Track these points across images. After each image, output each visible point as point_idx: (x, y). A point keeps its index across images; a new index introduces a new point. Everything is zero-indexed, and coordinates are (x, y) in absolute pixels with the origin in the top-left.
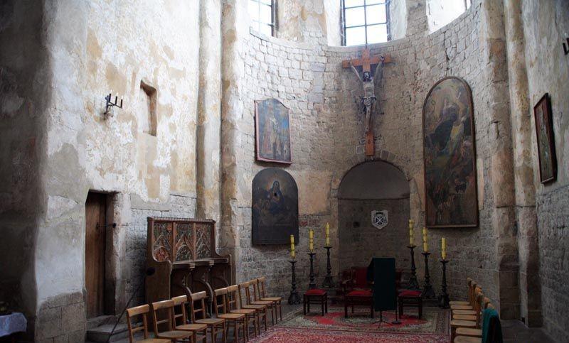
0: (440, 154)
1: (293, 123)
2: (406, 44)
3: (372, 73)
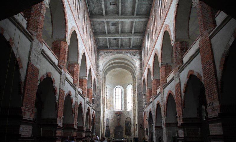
1: (109, 121)
2: (123, 111)
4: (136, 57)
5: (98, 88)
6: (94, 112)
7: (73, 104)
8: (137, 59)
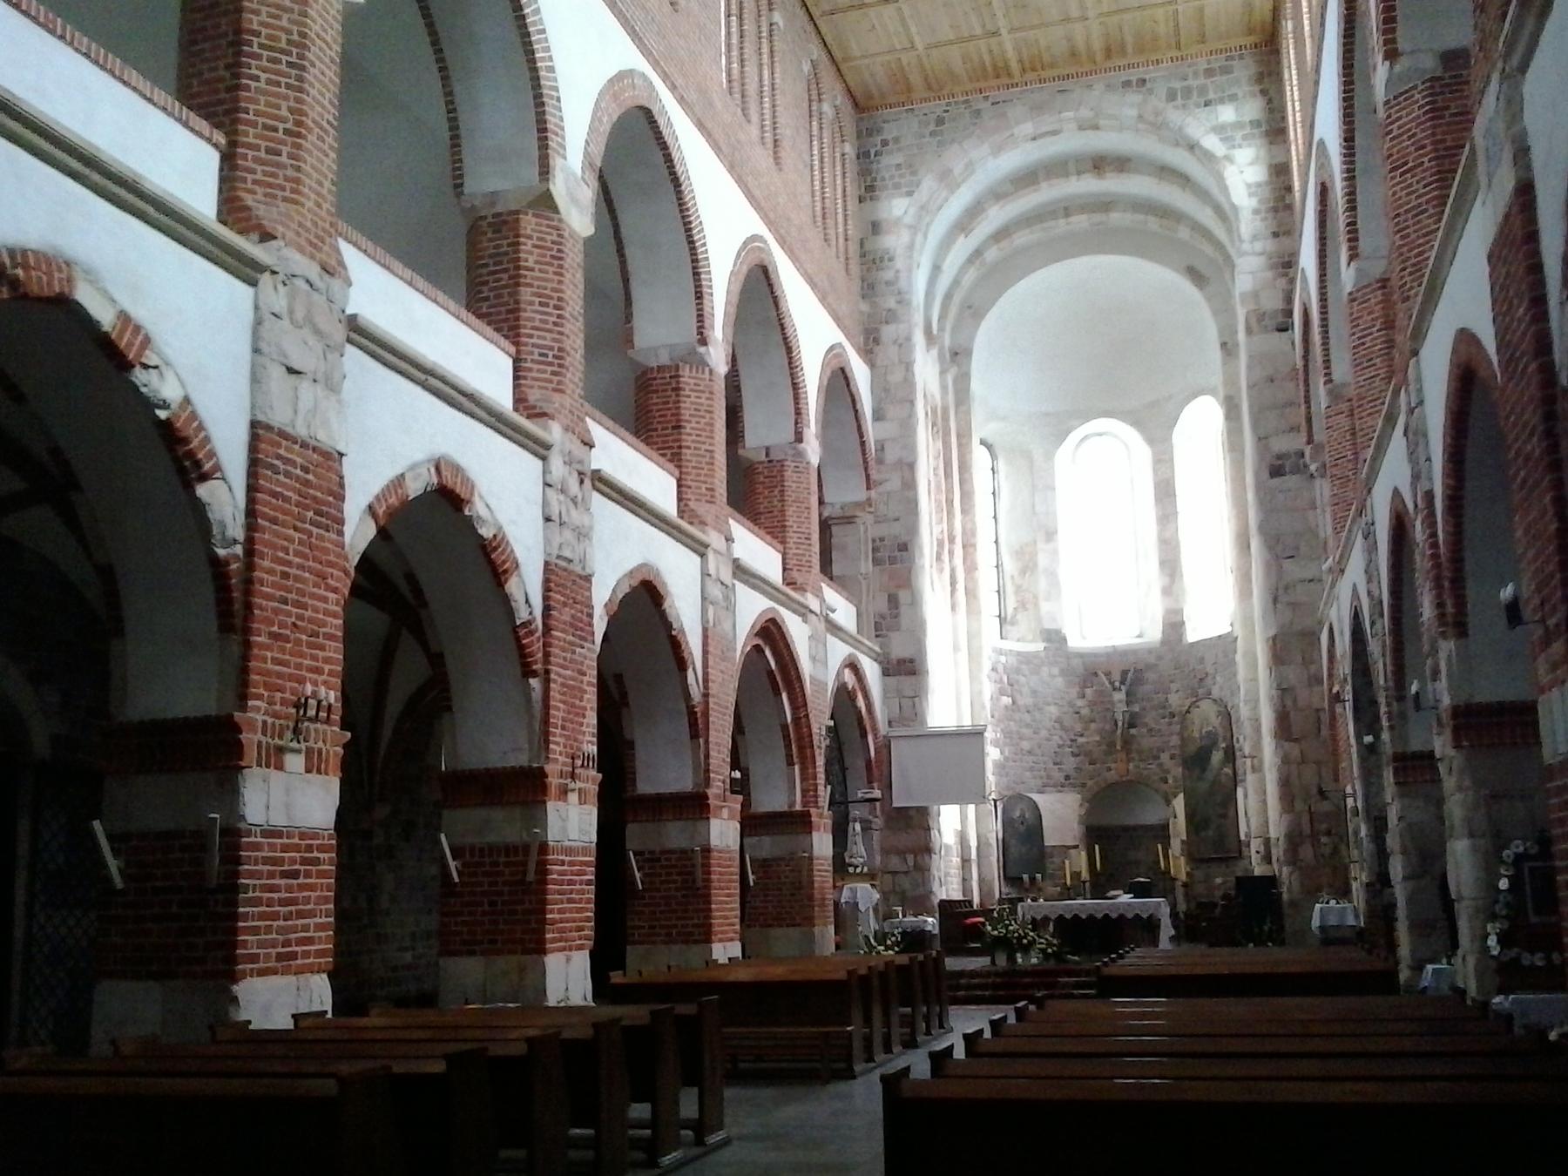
0: (1200, 779)
3: (1122, 683)
4: (1227, 114)
5: (891, 455)
6: (853, 666)
7: (527, 586)
8: (1239, 135)
